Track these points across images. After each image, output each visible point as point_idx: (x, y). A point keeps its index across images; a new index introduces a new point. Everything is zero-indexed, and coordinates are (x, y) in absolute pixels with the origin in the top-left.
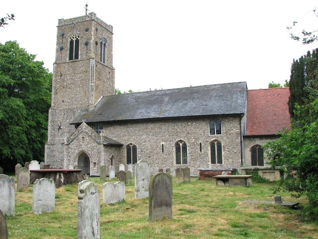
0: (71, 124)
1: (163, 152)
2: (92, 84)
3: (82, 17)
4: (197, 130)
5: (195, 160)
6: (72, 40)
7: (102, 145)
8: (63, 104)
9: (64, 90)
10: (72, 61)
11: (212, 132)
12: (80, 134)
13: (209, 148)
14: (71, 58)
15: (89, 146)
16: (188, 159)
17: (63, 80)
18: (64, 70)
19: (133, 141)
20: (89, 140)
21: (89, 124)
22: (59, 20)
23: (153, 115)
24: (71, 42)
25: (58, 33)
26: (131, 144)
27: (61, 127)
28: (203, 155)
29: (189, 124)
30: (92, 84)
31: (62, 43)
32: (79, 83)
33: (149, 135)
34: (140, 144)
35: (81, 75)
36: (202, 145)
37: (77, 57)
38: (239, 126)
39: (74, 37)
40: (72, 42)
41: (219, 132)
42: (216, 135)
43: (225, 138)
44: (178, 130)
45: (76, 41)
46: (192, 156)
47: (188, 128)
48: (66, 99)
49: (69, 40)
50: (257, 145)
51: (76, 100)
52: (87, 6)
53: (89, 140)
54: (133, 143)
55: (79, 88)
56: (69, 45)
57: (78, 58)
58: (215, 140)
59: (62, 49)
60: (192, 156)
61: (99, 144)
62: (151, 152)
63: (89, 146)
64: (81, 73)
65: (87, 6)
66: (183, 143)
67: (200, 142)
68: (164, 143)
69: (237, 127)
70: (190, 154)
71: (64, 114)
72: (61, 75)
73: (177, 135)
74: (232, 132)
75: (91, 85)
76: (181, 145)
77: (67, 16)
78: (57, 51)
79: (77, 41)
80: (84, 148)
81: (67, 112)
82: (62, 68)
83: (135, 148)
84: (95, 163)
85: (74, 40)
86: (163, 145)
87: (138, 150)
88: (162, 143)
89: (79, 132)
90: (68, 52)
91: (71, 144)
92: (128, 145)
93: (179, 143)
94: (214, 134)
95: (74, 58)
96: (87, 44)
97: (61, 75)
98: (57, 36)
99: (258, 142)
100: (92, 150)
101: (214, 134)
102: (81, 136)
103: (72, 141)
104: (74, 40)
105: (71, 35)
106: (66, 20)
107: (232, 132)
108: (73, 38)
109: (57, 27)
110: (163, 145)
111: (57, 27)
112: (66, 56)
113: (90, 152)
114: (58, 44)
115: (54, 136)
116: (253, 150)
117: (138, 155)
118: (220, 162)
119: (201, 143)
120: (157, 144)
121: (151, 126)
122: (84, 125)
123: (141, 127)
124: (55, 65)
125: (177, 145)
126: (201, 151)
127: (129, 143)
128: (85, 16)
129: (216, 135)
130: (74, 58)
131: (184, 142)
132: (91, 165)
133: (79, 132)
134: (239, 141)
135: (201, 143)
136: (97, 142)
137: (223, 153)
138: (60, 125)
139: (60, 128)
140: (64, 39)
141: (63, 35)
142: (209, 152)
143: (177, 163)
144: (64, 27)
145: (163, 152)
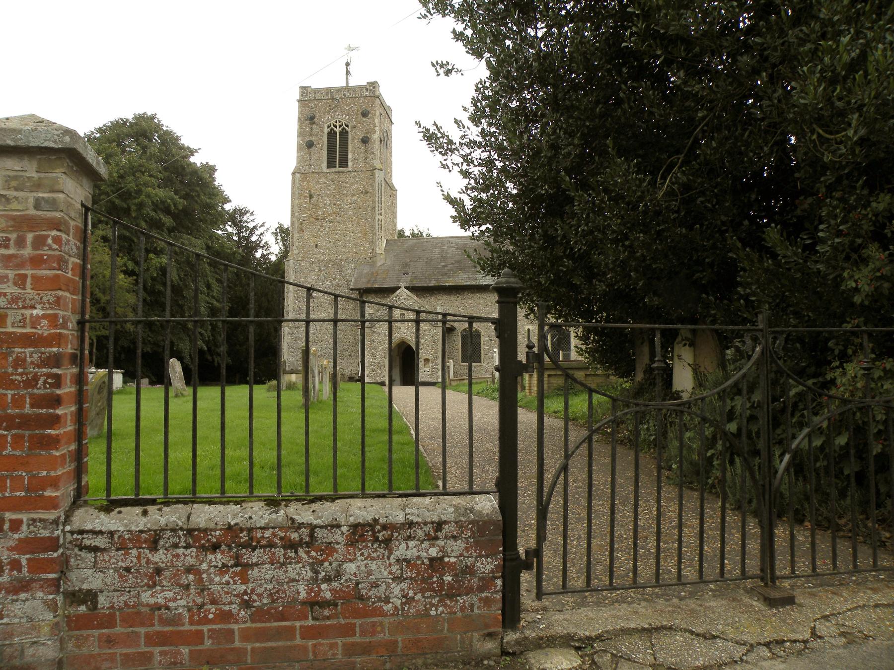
2: (380, 217)
3: (339, 90)
6: (332, 129)
8: (316, 250)
9: (318, 224)
10: (333, 170)
14: (331, 164)
21: (412, 289)
22: (301, 87)
24: (329, 133)
25: (300, 113)
31: (311, 135)
32: (351, 212)
37: (344, 163)
39: (338, 124)
40: (331, 134)
45: (340, 133)
48: (322, 243)
49: (326, 130)
52: (348, 64)
56: (325, 139)
59: (310, 145)
64: (354, 195)
65: (348, 64)
71: (320, 270)
72: (311, 197)
77: (317, 83)
78: (300, 148)
79: (344, 133)
81: (327, 267)
84: (427, 360)
85: (338, 130)
88: (527, 328)
90: (325, 153)
96: (365, 141)
97: (311, 197)
98: (299, 119)
104: (338, 130)
105: (326, 121)
106: (316, 91)
109: (298, 101)
111: (298, 101)
112: (319, 159)
114: (301, 134)
122: (403, 293)
124: (298, 175)
140: (314, 126)
141: (312, 119)
144: (314, 104)
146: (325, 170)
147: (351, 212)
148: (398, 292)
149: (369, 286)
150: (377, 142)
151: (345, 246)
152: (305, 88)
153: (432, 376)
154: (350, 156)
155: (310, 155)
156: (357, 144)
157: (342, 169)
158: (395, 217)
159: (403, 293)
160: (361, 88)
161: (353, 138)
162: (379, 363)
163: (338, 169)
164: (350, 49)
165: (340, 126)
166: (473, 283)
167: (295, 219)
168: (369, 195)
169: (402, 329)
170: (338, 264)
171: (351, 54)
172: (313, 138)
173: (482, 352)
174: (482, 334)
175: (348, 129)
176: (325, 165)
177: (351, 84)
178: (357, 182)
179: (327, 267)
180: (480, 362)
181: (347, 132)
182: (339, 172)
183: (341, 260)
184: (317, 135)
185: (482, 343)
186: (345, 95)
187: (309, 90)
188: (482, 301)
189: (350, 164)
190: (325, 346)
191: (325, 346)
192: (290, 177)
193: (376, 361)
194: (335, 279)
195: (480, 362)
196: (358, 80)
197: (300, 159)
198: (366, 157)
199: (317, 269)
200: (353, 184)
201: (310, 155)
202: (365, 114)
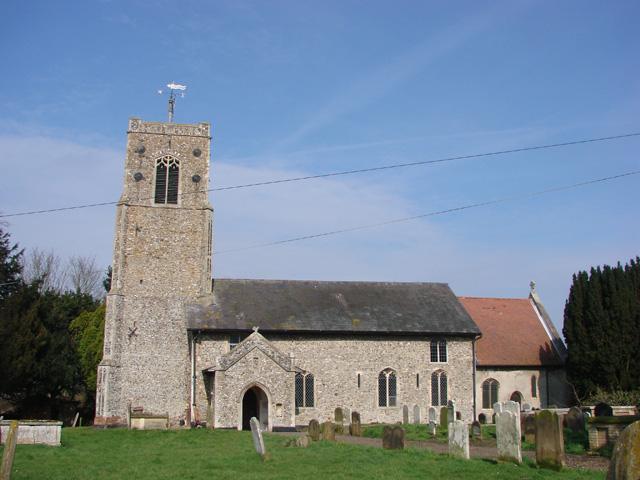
10: (162, 205)
11: (434, 359)
14: (159, 200)
15: (268, 374)
16: (398, 399)
17: (142, 240)
18: (145, 221)
19: (307, 367)
27: (136, 332)
31: (140, 167)
32: (178, 251)
33: (337, 358)
34: (321, 373)
36: (421, 377)
37: (173, 198)
38: (471, 351)
39: (168, 160)
40: (161, 170)
41: (443, 359)
43: (452, 368)
45: (170, 168)
47: (400, 351)
49: (156, 165)
50: (491, 379)
51: (171, 282)
54: (308, 369)
58: (440, 370)
59: (139, 177)
63: (268, 374)
64: (182, 233)
67: (418, 372)
68: (361, 373)
76: (387, 376)
79: (174, 171)
80: (257, 378)
85: (168, 165)
96: (196, 179)
99: (492, 374)
102: (250, 356)
104: (168, 165)
115: (119, 348)
116: (485, 386)
117: (317, 392)
121: (340, 343)
122: (256, 337)
125: (382, 375)
126: (418, 385)
134: (470, 372)
137: (449, 389)
140: (144, 159)
141: (142, 151)
142: (430, 388)
143: (380, 405)
146: (154, 205)
147: (178, 251)
149: (206, 326)
151: (171, 282)
153: (284, 420)
154: (180, 192)
155: (138, 187)
157: (171, 206)
159: (256, 337)
161: (184, 176)
163: (166, 205)
165: (171, 162)
166: (309, 329)
167: (120, 252)
173: (315, 397)
174: (315, 379)
175: (180, 166)
181: (177, 169)
188: (315, 346)
189: (179, 201)
193: (229, 405)
199: (141, 306)
200: (182, 221)
202: (197, 153)
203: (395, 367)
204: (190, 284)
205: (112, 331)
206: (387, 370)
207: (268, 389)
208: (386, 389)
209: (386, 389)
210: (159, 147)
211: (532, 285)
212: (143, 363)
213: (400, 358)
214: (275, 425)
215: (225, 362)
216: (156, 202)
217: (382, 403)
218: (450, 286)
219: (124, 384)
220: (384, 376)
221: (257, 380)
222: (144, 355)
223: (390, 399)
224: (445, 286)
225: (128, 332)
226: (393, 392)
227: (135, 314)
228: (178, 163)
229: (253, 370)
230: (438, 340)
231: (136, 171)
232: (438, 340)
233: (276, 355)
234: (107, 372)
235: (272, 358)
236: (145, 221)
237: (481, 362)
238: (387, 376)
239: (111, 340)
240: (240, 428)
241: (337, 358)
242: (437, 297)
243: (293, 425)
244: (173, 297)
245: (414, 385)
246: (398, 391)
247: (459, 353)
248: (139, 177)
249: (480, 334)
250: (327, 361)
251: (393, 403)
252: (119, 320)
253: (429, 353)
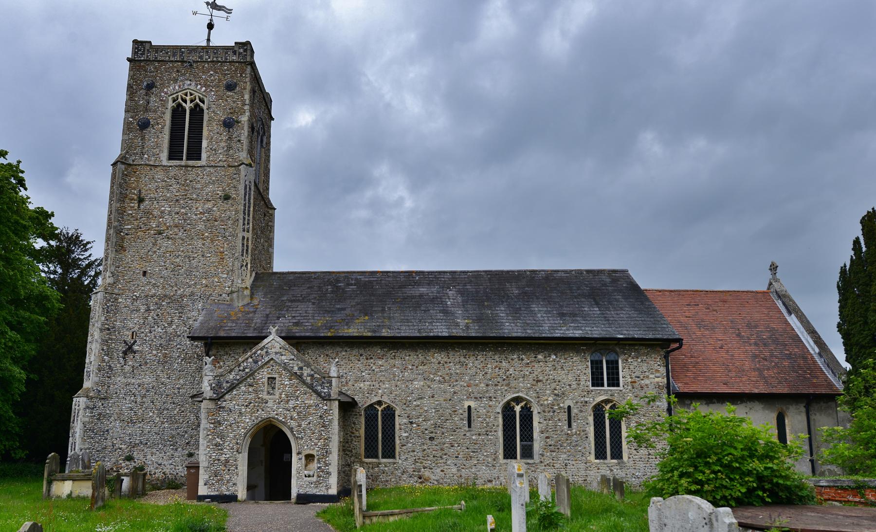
0: (193, 338)
1: (469, 426)
2: (246, 235)
4: (561, 375)
5: (554, 448)
6: (179, 105)
7: (337, 402)
8: (143, 279)
11: (597, 381)
12: (262, 367)
13: (591, 419)
14: (175, 154)
15: (291, 404)
16: (537, 446)
17: (148, 213)
18: (153, 186)
20: (291, 386)
23: (406, 331)
25: (132, 77)
26: (379, 403)
28: (574, 438)
29: (540, 357)
30: (246, 235)
32: (201, 226)
33: (433, 380)
34: (407, 404)
35: (209, 205)
36: (574, 411)
37: (195, 153)
38: (663, 370)
39: (188, 98)
40: (178, 113)
41: (614, 381)
42: (606, 387)
44: (511, 371)
45: (191, 110)
46: (547, 438)
47: (538, 368)
49: (170, 104)
51: (189, 273)
52: (210, 26)
53: (291, 386)
54: (385, 399)
55: (200, 242)
56: (168, 117)
57: (199, 158)
58: (607, 401)
60: (547, 438)
61: (327, 398)
62: (436, 426)
63: (291, 404)
65: (210, 26)
66: (523, 404)
68: (472, 404)
69: (657, 371)
70: (542, 432)
71: (148, 310)
73: (508, 385)
74: (647, 382)
75: (243, 238)
76: (518, 409)
79: (197, 112)
80: (274, 409)
81: (159, 306)
82: (144, 180)
83: (389, 414)
84: (309, 458)
85: (188, 106)
86: (469, 407)
87: (398, 420)
88: (466, 404)
89: (256, 362)
91: (227, 397)
92: (371, 405)
93: (513, 404)
94: (603, 385)
95: (184, 158)
97: (141, 200)
100: (302, 416)
101: (603, 385)
102: (263, 376)
103: (230, 390)
104: (188, 106)
107: (647, 382)
108: (185, 101)
110: (469, 407)
111: (129, 59)
113: (293, 424)
117: (400, 434)
118: (617, 454)
119: (569, 407)
120: (453, 406)
121: (437, 357)
122: (273, 342)
123: (411, 358)
124: (119, 165)
125: (508, 411)
126: (570, 426)
127: (375, 399)
128: (203, 48)
129: (606, 387)
130: (184, 158)
131: (528, 402)
132: (296, 463)
133: (256, 362)
135: (569, 407)
136: (319, 394)
138: (129, 339)
139: (129, 350)
142: (591, 430)
143: (506, 457)
145: (469, 426)
146: (165, 162)
148: (266, 341)
150: (246, 128)
151: (189, 273)
152: (142, 43)
153: (317, 484)
154: (205, 144)
156: (215, 127)
157: (191, 163)
158: (271, 245)
160: (226, 49)
162: (227, 461)
163: (183, 163)
164: (214, 6)
165: (192, 101)
167: (111, 232)
168: (230, 202)
169: (270, 404)
170: (177, 302)
171: (215, 12)
172: (150, 116)
173: (397, 442)
174: (397, 413)
175: (205, 107)
176: (164, 155)
177: (214, 43)
178: (213, 183)
179: (159, 306)
180: (394, 457)
181: (202, 110)
182: (186, 166)
183: (182, 296)
184: (155, 111)
185: (397, 427)
186: (201, 57)
187: (147, 46)
188: (398, 362)
189: (204, 155)
190: (147, 428)
191: (147, 428)
192: (110, 169)
194: (170, 324)
195: (394, 457)
196: (220, 39)
197: (127, 146)
198: (229, 148)
201: (143, 139)
202: (230, 87)
203: (531, 397)
204: (216, 275)
205: (93, 347)
206: (518, 400)
207: (291, 429)
208: (517, 430)
209: (517, 430)
210: (175, 80)
211: (774, 268)
212: (143, 392)
213: (538, 381)
214: (302, 491)
215: (219, 385)
216: (171, 158)
217: (509, 453)
218: (631, 273)
219: (115, 427)
220: (512, 409)
221: (273, 414)
222: (148, 380)
223: (523, 448)
224: (624, 272)
225: (122, 348)
226: (527, 435)
227: (134, 322)
228: (203, 102)
229: (265, 396)
230: (604, 356)
231: (141, 116)
232: (604, 356)
233: (306, 371)
234: (82, 406)
235: (300, 377)
236: (153, 186)
237: (679, 387)
238: (518, 409)
239: (92, 359)
240: (242, 494)
241: (433, 380)
242: (612, 288)
243: (333, 491)
244: (192, 294)
245: (566, 427)
246: (536, 435)
247: (641, 376)
248: (144, 125)
249: (679, 341)
250: (417, 384)
251: (528, 453)
252: (108, 329)
253: (589, 371)
